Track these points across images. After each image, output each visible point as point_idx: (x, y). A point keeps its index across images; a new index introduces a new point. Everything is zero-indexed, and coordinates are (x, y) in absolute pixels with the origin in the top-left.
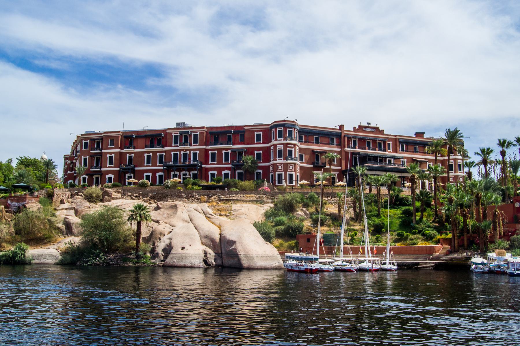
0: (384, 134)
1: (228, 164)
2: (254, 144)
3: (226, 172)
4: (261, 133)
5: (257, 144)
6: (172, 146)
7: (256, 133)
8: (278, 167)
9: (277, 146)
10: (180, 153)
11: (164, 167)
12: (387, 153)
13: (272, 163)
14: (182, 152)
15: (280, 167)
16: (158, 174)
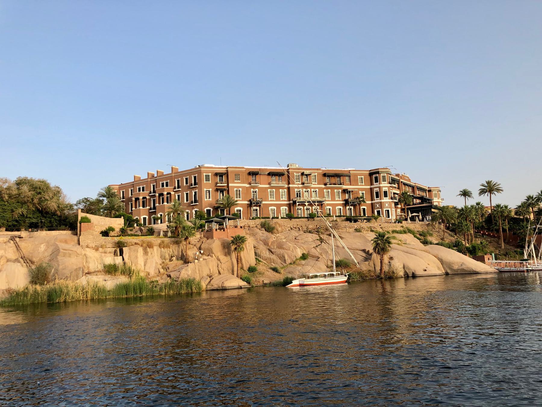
0: (410, 182)
1: (340, 201)
2: (358, 185)
3: (340, 207)
4: (363, 177)
5: (361, 185)
7: (359, 177)
13: (376, 201)
15: (387, 204)
16: (281, 208)
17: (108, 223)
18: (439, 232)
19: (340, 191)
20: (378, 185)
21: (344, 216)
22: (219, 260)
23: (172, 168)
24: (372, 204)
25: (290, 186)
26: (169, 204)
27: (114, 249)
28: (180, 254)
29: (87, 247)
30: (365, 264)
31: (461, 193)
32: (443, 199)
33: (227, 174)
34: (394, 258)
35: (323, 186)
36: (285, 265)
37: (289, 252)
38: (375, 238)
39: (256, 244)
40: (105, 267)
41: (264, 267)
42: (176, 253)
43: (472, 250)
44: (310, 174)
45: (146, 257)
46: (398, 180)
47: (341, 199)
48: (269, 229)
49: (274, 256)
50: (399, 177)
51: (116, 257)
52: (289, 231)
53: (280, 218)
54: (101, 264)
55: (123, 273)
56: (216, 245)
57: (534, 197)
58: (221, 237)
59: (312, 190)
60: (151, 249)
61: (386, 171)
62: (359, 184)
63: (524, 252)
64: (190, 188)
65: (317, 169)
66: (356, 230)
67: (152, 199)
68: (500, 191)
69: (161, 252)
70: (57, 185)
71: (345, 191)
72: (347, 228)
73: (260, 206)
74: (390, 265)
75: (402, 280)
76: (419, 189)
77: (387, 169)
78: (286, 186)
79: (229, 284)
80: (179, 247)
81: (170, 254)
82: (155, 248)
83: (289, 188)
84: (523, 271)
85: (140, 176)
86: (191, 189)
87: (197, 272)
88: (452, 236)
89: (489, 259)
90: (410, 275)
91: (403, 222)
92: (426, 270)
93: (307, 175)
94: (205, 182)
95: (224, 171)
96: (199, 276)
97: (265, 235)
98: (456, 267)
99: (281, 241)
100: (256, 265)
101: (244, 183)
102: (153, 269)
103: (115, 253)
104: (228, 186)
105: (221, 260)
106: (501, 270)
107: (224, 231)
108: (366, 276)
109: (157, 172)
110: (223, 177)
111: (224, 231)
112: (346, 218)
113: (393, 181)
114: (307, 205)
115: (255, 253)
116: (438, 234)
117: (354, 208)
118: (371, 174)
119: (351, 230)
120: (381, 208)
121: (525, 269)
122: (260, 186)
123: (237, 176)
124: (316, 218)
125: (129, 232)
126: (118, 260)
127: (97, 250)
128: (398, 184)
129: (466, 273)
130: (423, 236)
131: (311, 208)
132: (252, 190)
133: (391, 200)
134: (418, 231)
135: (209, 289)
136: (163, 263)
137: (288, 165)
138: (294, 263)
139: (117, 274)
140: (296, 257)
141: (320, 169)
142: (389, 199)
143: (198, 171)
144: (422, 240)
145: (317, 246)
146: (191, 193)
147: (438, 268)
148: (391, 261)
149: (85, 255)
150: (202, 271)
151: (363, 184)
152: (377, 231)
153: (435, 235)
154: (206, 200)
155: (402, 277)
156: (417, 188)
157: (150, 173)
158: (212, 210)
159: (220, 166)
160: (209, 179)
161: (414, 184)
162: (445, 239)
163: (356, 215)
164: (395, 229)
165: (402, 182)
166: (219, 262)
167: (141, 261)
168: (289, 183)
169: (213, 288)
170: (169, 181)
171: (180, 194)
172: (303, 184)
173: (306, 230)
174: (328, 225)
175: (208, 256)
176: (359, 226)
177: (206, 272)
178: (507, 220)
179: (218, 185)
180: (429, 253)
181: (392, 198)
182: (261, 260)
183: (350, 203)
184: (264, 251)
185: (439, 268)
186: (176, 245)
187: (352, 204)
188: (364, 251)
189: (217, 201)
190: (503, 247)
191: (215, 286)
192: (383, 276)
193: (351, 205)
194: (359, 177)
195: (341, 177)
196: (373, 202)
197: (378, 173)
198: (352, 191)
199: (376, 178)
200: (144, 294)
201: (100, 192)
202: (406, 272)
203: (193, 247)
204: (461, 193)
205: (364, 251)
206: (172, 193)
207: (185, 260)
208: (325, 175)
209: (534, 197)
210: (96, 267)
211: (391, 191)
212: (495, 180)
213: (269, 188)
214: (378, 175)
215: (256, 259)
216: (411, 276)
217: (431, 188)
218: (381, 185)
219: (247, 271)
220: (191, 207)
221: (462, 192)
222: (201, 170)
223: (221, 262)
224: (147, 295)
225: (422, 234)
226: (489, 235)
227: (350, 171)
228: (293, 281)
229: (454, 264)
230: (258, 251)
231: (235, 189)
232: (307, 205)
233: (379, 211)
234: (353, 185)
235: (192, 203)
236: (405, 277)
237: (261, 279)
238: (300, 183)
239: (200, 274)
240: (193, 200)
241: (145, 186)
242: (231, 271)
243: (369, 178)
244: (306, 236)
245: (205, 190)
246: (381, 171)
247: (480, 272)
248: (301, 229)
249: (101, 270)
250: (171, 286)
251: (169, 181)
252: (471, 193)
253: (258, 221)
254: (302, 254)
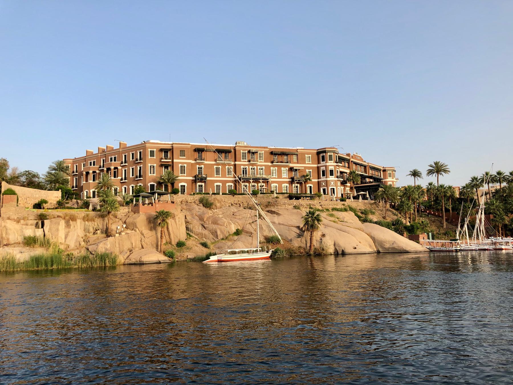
2: (305, 164)
4: (310, 156)
6: (241, 161)
7: (306, 155)
8: (331, 183)
9: (329, 167)
10: (249, 167)
13: (322, 179)
15: (332, 183)
17: (45, 196)
18: (382, 211)
19: (287, 168)
20: (325, 164)
21: (287, 193)
22: (143, 234)
23: (120, 143)
24: (318, 182)
25: (237, 163)
26: (116, 178)
27: (36, 221)
28: (105, 227)
29: (9, 218)
30: (297, 240)
31: (411, 173)
32: (397, 179)
33: (172, 150)
34: (326, 235)
35: (270, 164)
36: (216, 241)
37: (222, 227)
38: (306, 215)
39: (190, 219)
40: (25, 239)
41: (194, 242)
42: (101, 227)
43: (411, 229)
44: (257, 152)
45: (67, 230)
46: (348, 159)
47: (287, 177)
48: (207, 205)
49: (206, 231)
50: (349, 157)
51: (37, 230)
52: (229, 207)
53: (221, 193)
54: (21, 236)
55: (42, 245)
56: (141, 219)
57: (479, 178)
58: (149, 211)
59: (259, 167)
60: (75, 222)
61: (332, 151)
62: (307, 162)
63: (457, 231)
64: (136, 162)
65: (265, 148)
66: (295, 207)
67: (101, 173)
68: (448, 172)
69: (85, 226)
70: (4, 158)
71: (291, 169)
72: (286, 205)
73: (205, 182)
74: (321, 242)
75: (333, 257)
76: (372, 169)
77: (334, 148)
78: (233, 163)
79: (147, 259)
80: (103, 220)
81: (95, 227)
82: (79, 221)
83: (235, 165)
84: (452, 251)
85: (93, 151)
86: (137, 164)
87: (117, 246)
88: (395, 214)
89: (424, 238)
90: (340, 252)
91: (347, 200)
92: (355, 248)
93: (253, 153)
94: (149, 157)
95: (169, 147)
96: (119, 250)
97: (201, 211)
98: (387, 246)
99: (216, 217)
100: (186, 240)
101: (189, 159)
102: (74, 242)
103: (37, 226)
104: (173, 162)
105: (144, 234)
106: (432, 249)
107: (152, 205)
108: (295, 253)
109: (107, 147)
110: (168, 153)
111: (152, 205)
112: (288, 195)
113: (341, 159)
114: (251, 182)
115: (187, 228)
116: (381, 213)
117: (300, 186)
118: (318, 153)
119: (290, 207)
120: (327, 186)
121: (454, 248)
122: (206, 162)
123: (182, 153)
124: (259, 195)
125: (67, 205)
126: (39, 233)
127: (18, 222)
128: (348, 163)
129: (397, 251)
130: (365, 214)
131: (256, 185)
132: (198, 166)
133: (337, 179)
134: (360, 210)
135: (126, 263)
136: (86, 235)
137: (236, 142)
138: (226, 238)
139: (36, 246)
140: (229, 232)
141: (267, 148)
142: (335, 177)
143: (143, 146)
144: (363, 218)
145: (253, 222)
146: (136, 168)
147: (370, 246)
148: (322, 238)
149: (5, 226)
150: (123, 245)
151: (311, 163)
152: (316, 208)
153: (377, 213)
154: (150, 175)
155: (331, 255)
156: (370, 168)
157: (101, 148)
158: (156, 185)
159: (166, 143)
160: (154, 154)
161: (367, 164)
162: (387, 218)
163: (302, 192)
164: (335, 206)
165: (352, 161)
166: (142, 237)
167: (62, 234)
168: (235, 161)
169: (130, 262)
170: (116, 156)
171: (126, 169)
172: (249, 161)
173: (246, 206)
174: (253, 202)
175: (132, 230)
176: (298, 203)
177: (127, 246)
178: (450, 200)
179: (162, 160)
180: (363, 231)
181: (337, 177)
182: (193, 235)
183: (296, 181)
184: (197, 227)
185: (370, 246)
186: (101, 219)
187: (297, 181)
188: (298, 227)
189: (161, 177)
190: (445, 227)
191: (133, 261)
192: (312, 253)
193: (297, 183)
194: (306, 155)
195: (289, 156)
196: (320, 180)
197: (325, 152)
198: (299, 169)
199: (323, 157)
200: (55, 267)
201: (50, 166)
202: (336, 249)
203: (118, 221)
204: (411, 173)
205: (298, 227)
206: (119, 168)
207: (108, 233)
208: (272, 153)
209: (479, 178)
210: (16, 239)
211: (337, 169)
212: (442, 161)
213: (215, 165)
214: (325, 154)
215: (187, 233)
216: (341, 253)
217: (385, 168)
218: (327, 164)
219: (175, 246)
220: (136, 182)
221: (411, 172)
222: (146, 146)
223: (144, 237)
224: (58, 268)
225: (365, 212)
226: (434, 215)
227: (297, 149)
228: (211, 257)
229: (385, 242)
230: (190, 226)
231: (180, 165)
232: (251, 182)
233: (325, 189)
234: (300, 164)
235: (137, 178)
236: (335, 254)
237: (186, 254)
238: (247, 160)
239: (119, 248)
240: (138, 175)
241: (95, 160)
242: (155, 246)
243: (316, 157)
244: (244, 212)
245: (149, 165)
246: (328, 151)
247: (409, 251)
248: (241, 205)
249: (21, 242)
250: (84, 259)
251: (116, 156)
252: (421, 174)
253: (197, 197)
254: (236, 230)
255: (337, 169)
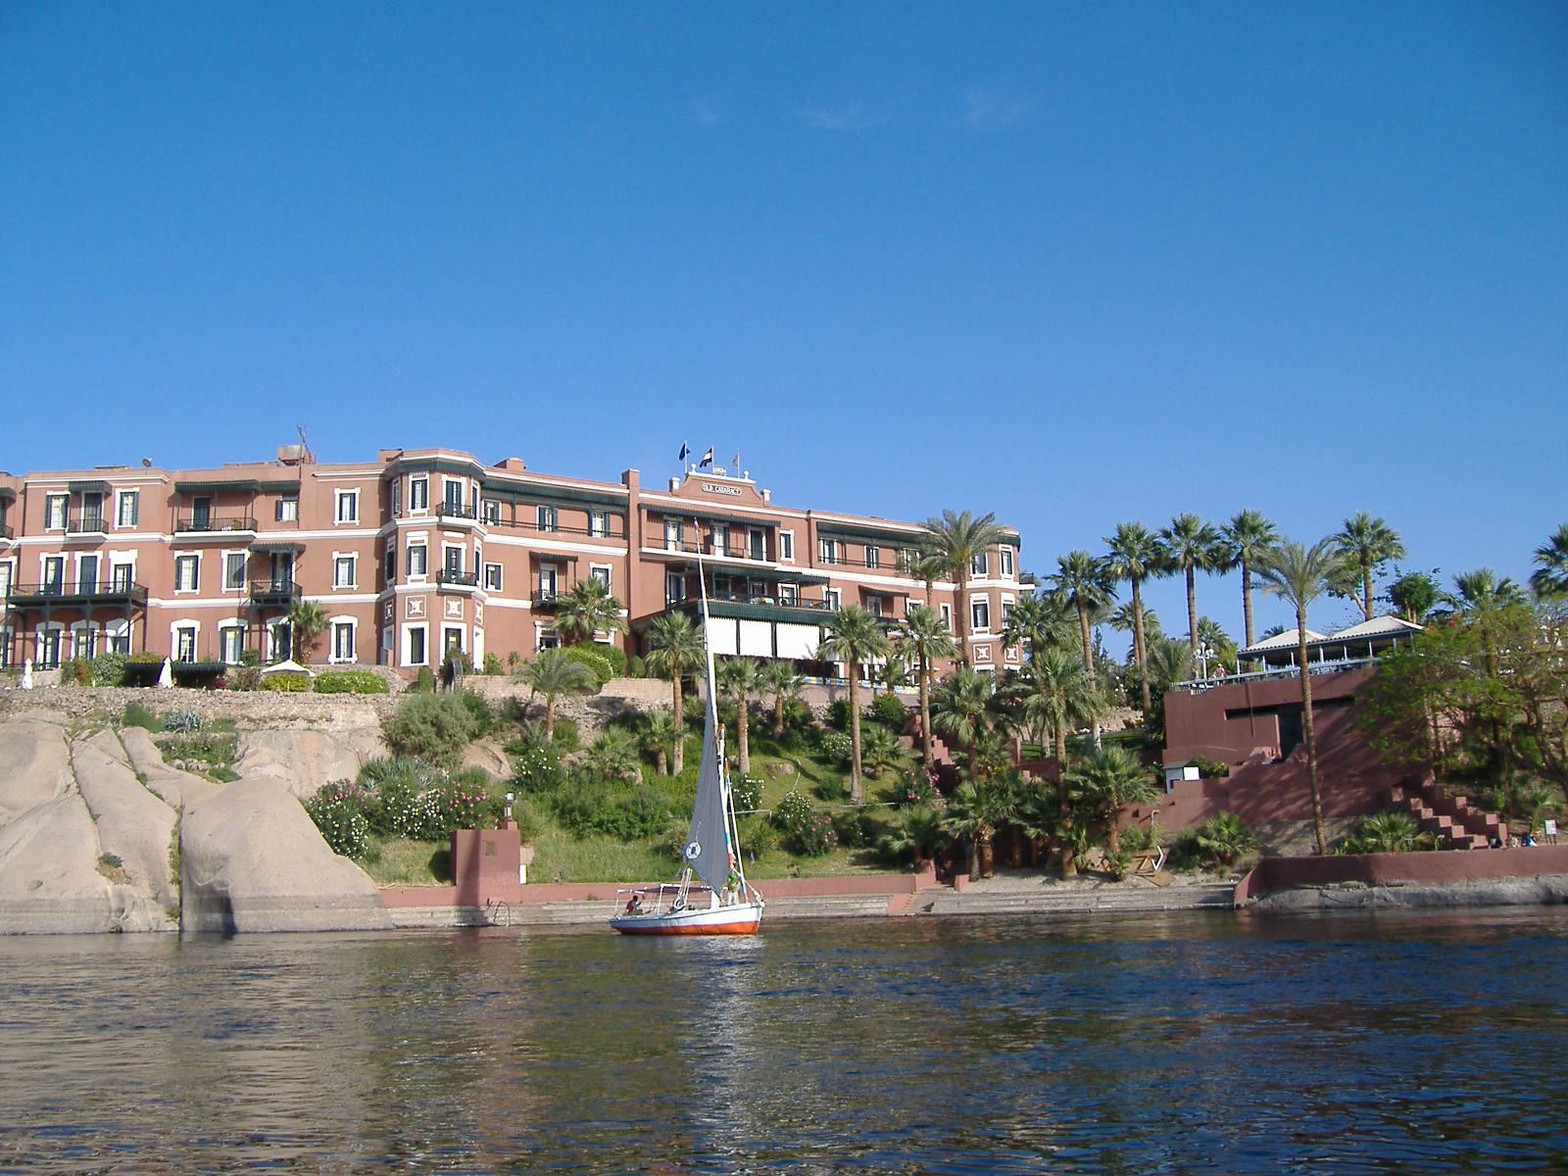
9: (408, 534)
11: (11, 606)
12: (779, 567)
14: (78, 555)
19: (247, 554)
255: (445, 544)
